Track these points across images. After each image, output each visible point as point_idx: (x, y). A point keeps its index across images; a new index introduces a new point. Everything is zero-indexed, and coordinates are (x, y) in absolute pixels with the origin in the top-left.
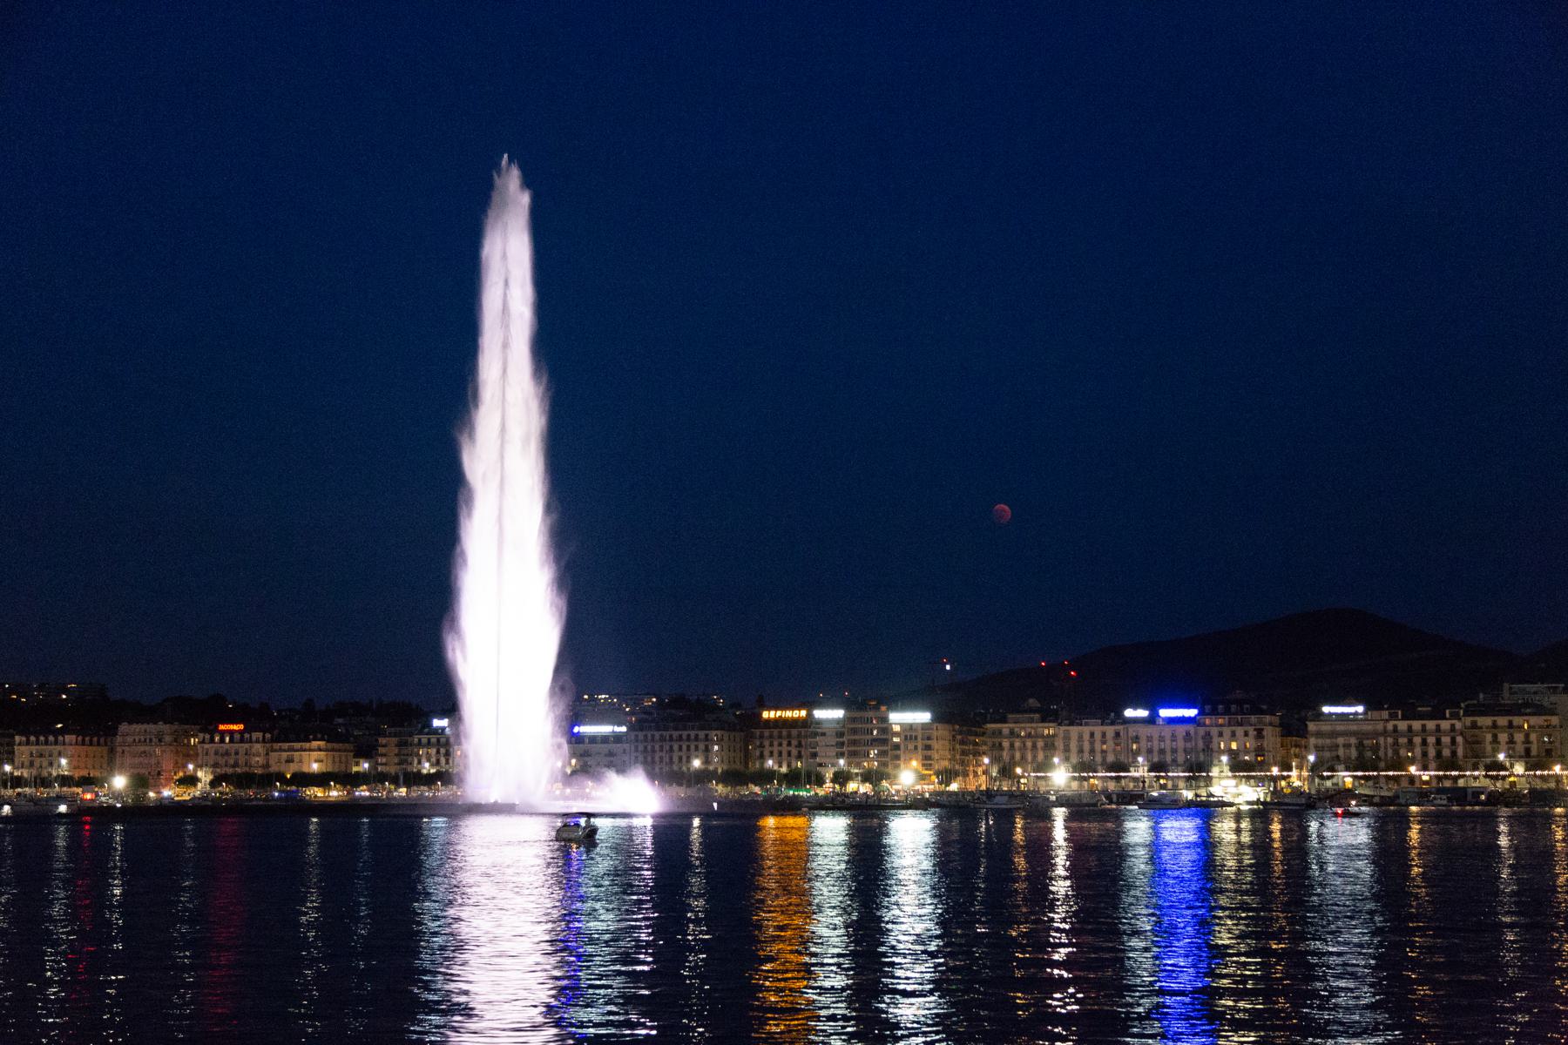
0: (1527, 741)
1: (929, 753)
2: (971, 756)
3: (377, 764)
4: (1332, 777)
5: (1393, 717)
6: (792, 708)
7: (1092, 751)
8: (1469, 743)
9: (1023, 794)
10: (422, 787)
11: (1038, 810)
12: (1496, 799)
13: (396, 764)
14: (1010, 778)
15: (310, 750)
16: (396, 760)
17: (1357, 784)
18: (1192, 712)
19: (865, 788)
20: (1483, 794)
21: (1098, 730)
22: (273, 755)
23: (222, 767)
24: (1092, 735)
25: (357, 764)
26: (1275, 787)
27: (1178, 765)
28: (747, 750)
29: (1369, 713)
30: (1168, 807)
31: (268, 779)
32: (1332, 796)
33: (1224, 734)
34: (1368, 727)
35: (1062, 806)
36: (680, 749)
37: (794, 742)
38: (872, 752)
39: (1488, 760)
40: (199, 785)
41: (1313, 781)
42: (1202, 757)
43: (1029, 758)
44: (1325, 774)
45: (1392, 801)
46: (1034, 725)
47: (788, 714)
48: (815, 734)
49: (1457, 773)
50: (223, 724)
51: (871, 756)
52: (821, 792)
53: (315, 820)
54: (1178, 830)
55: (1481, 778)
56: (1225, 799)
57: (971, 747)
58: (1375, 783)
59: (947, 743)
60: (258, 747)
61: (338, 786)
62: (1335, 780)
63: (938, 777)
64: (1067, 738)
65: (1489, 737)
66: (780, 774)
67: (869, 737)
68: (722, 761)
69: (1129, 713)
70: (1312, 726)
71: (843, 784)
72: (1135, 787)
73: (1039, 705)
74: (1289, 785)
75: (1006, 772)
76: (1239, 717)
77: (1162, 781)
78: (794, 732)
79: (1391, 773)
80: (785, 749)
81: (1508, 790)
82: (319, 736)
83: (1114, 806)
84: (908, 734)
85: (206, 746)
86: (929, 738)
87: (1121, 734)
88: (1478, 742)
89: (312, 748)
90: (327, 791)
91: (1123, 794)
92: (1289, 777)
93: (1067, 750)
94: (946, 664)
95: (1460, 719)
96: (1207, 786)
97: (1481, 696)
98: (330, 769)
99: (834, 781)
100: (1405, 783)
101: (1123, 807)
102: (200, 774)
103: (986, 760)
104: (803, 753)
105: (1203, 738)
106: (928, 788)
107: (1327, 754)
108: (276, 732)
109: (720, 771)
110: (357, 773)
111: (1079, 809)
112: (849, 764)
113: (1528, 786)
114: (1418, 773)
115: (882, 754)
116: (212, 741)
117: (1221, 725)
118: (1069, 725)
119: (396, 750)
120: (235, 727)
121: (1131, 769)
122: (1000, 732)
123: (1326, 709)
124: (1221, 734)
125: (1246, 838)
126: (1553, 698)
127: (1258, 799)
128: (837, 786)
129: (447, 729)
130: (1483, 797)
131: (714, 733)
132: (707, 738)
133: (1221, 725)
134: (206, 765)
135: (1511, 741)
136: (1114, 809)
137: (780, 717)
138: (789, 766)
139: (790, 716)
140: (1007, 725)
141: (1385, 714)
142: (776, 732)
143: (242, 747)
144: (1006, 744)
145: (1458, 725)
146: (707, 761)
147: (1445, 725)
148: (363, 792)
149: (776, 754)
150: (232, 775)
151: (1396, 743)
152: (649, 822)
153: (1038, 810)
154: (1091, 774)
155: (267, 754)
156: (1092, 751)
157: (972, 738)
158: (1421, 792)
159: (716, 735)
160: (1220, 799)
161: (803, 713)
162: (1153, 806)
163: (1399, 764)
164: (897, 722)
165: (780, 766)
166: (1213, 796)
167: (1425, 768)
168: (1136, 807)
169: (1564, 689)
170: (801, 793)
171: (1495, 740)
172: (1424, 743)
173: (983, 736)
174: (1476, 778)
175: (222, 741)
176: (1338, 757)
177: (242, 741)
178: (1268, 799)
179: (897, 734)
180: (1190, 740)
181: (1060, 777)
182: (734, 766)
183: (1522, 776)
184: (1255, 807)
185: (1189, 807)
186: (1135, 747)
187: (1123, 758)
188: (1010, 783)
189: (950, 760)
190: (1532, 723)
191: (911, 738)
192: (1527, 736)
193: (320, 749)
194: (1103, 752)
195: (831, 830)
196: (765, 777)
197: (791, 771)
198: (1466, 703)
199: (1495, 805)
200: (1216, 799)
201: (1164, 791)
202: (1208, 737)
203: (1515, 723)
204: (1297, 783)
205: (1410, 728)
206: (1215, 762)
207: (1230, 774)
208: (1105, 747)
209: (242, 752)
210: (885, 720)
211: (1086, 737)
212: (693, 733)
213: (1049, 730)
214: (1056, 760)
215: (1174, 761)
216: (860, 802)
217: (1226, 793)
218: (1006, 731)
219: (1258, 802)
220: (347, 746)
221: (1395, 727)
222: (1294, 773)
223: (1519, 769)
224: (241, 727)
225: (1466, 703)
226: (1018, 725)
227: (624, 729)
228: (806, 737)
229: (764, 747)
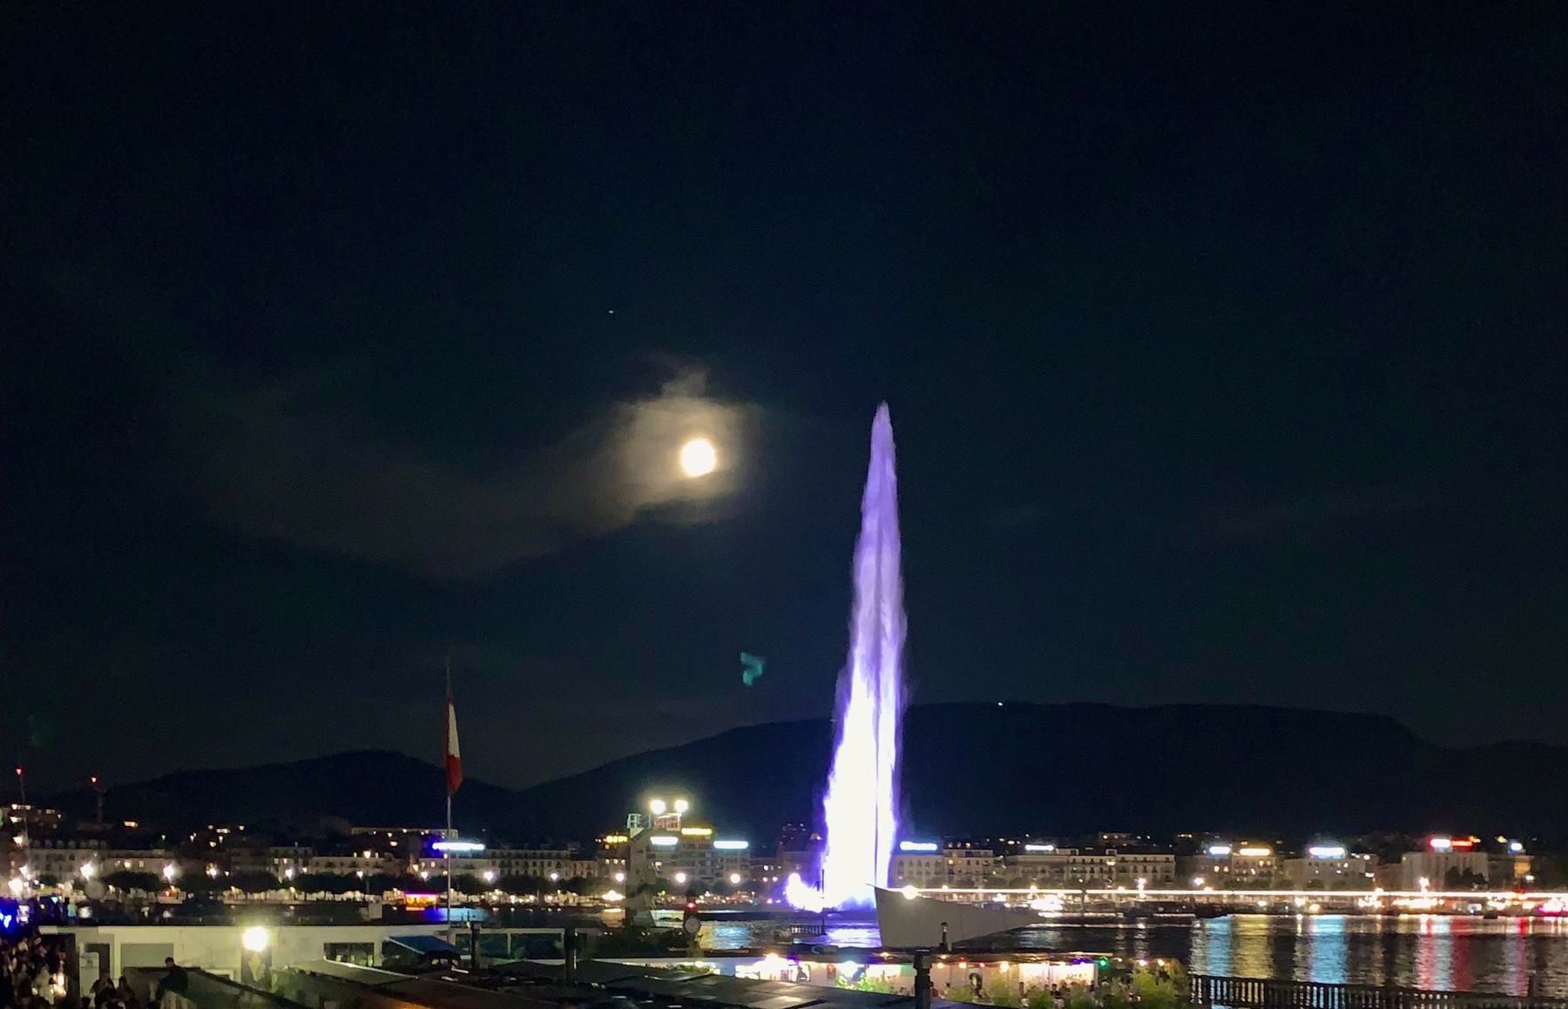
5: (1073, 854)
33: (971, 863)
34: (1057, 859)
36: (535, 864)
65: (1132, 868)
141: (1068, 851)
229: (528, 866)
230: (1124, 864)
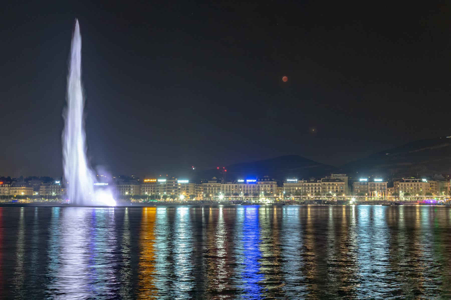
0: (337, 188)
1: (188, 191)
2: (199, 192)
3: (40, 193)
4: (289, 197)
5: (305, 182)
6: (152, 179)
7: (230, 190)
8: (323, 189)
9: (212, 201)
10: (52, 199)
11: (216, 206)
12: (329, 203)
13: (45, 193)
14: (208, 197)
16: (45, 192)
17: (295, 199)
18: (255, 181)
19: (171, 200)
20: (326, 201)
21: (231, 185)
24: (230, 186)
25: (34, 193)
26: (275, 200)
29: (299, 181)
32: (289, 202)
37: (153, 188)
38: (173, 190)
39: (327, 193)
41: (284, 198)
42: (257, 192)
43: (214, 192)
44: (287, 196)
45: (304, 203)
46: (215, 184)
47: (151, 180)
48: (158, 186)
49: (320, 196)
52: (159, 200)
54: (251, 210)
55: (326, 197)
57: (199, 189)
58: (300, 199)
59: (192, 188)
60: (7, 188)
61: (29, 199)
62: (290, 198)
64: (223, 187)
65: (328, 187)
66: (149, 196)
68: (134, 193)
69: (239, 181)
70: (284, 184)
71: (165, 199)
73: (217, 179)
74: (279, 199)
75: (208, 196)
76: (267, 182)
77: (247, 198)
78: (153, 185)
79: (303, 196)
80: (150, 190)
81: (332, 200)
82: (24, 185)
86: (188, 187)
87: (237, 186)
88: (325, 189)
89: (22, 189)
92: (279, 197)
93: (223, 190)
94: (193, 168)
95: (321, 183)
96: (258, 199)
97: (326, 177)
98: (27, 194)
99: (163, 198)
100: (307, 198)
104: (155, 190)
105: (258, 187)
107: (288, 191)
109: (133, 195)
110: (34, 195)
111: (227, 205)
112: (167, 194)
113: (337, 199)
114: (310, 196)
115: (176, 191)
117: (262, 184)
119: (45, 189)
121: (239, 195)
123: (288, 180)
124: (262, 186)
125: (268, 213)
126: (343, 178)
127: (271, 203)
129: (59, 184)
130: (326, 202)
132: (130, 187)
133: (262, 184)
135: (333, 188)
136: (235, 205)
137: (149, 181)
138: (151, 194)
140: (207, 184)
141: (303, 181)
144: (208, 188)
145: (320, 184)
146: (130, 193)
147: (317, 184)
148: (36, 200)
151: (305, 189)
153: (216, 206)
154: (229, 196)
155: (9, 190)
156: (230, 190)
158: (311, 201)
159: (132, 186)
161: (155, 180)
163: (305, 194)
165: (149, 194)
166: (260, 202)
167: (312, 195)
168: (240, 205)
169: (346, 175)
170: (154, 201)
171: (329, 188)
172: (312, 189)
174: (324, 198)
176: (291, 192)
178: (273, 203)
179: (180, 186)
181: (221, 197)
183: (335, 197)
184: (270, 205)
186: (240, 189)
187: (237, 192)
189: (193, 192)
190: (338, 184)
191: (183, 187)
192: (337, 187)
193: (24, 189)
195: (162, 212)
196: (144, 197)
197: (152, 195)
198: (322, 179)
199: (328, 204)
200: (260, 203)
202: (259, 187)
203: (334, 184)
204: (281, 199)
205: (309, 185)
206: (261, 193)
207: (264, 196)
208: (233, 189)
210: (176, 182)
211: (228, 187)
213: (218, 184)
214: (220, 193)
215: (250, 193)
218: (208, 185)
219: (271, 203)
220: (31, 188)
221: (305, 185)
222: (280, 196)
223: (335, 195)
225: (322, 179)
226: (210, 184)
230: (324, 186)
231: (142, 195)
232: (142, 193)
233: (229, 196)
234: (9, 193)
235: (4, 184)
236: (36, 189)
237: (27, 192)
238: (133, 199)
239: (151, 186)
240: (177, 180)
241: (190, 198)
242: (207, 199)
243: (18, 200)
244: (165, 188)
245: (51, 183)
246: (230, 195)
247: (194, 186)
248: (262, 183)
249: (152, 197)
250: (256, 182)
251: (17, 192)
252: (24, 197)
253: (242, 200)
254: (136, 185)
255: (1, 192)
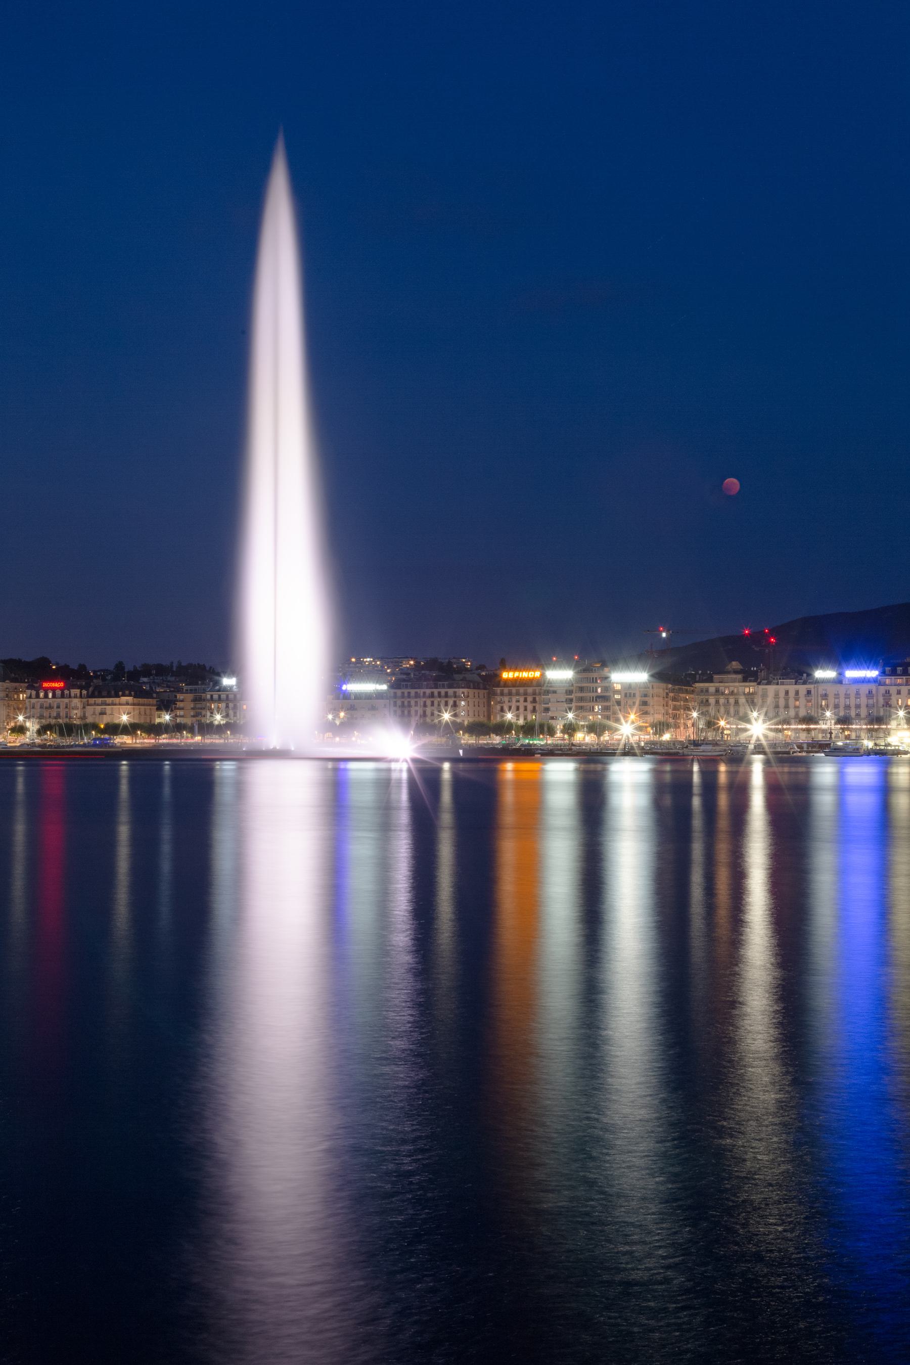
1: (645, 708)
6: (528, 670)
7: (787, 707)
15: (120, 704)
16: (192, 714)
21: (792, 688)
22: (90, 710)
23: (63, 718)
24: (787, 693)
25: (159, 717)
27: (861, 719)
28: (489, 705)
30: (849, 754)
31: (88, 727)
35: (759, 753)
36: (432, 704)
37: (530, 699)
38: (596, 707)
40: (28, 733)
42: (882, 714)
46: (737, 684)
47: (525, 675)
48: (547, 692)
50: (46, 682)
51: (596, 710)
53: (124, 762)
56: (901, 748)
57: (682, 703)
60: (76, 702)
61: (143, 735)
63: (652, 729)
66: (517, 726)
67: (594, 695)
69: (820, 674)
72: (823, 737)
73: (742, 668)
75: (710, 724)
78: (530, 690)
80: (522, 704)
82: (127, 692)
83: (804, 754)
84: (628, 692)
85: (33, 701)
86: (646, 696)
87: (812, 692)
90: (134, 738)
91: (813, 744)
94: (662, 632)
98: (135, 721)
99: (564, 731)
101: (812, 754)
102: (28, 724)
103: (695, 714)
104: (537, 708)
105: (883, 696)
106: (647, 737)
108: (91, 689)
109: (466, 723)
110: (160, 724)
115: (606, 708)
116: (38, 696)
117: (899, 685)
118: (767, 684)
120: (56, 685)
122: (707, 691)
124: (899, 693)
128: (566, 736)
131: (462, 690)
133: (899, 685)
134: (33, 717)
137: (518, 677)
138: (525, 719)
139: (526, 676)
142: (514, 690)
143: (47, 702)
144: (712, 700)
146: (455, 715)
149: (514, 708)
150: (55, 725)
152: (405, 766)
154: (785, 727)
155: (84, 707)
156: (787, 707)
157: (682, 695)
159: (463, 693)
160: (897, 748)
161: (537, 674)
162: (839, 754)
164: (619, 681)
168: (823, 755)
170: (535, 742)
173: (692, 694)
175: (46, 696)
177: (63, 696)
179: (618, 692)
180: (872, 697)
182: (477, 719)
185: (869, 754)
187: (813, 713)
188: (714, 733)
191: (630, 696)
193: (127, 704)
194: (796, 707)
196: (503, 729)
197: (526, 723)
200: (893, 748)
201: (848, 741)
207: (906, 726)
208: (797, 703)
209: (62, 706)
211: (782, 694)
212: (443, 691)
213: (750, 688)
215: (858, 715)
216: (585, 749)
217: (902, 743)
218: (712, 689)
220: (151, 701)
224: (62, 684)
227: (384, 687)
228: (540, 694)
231: (495, 722)
232: (495, 717)
233: (785, 727)
234: (84, 717)
235: (68, 690)
236: (166, 705)
237: (137, 712)
238: (467, 736)
239: (526, 694)
240: (610, 672)
241: (651, 731)
242: (710, 736)
243: (110, 739)
244: (571, 700)
245: (209, 684)
246: (789, 723)
247: (667, 691)
248: (899, 681)
249: (529, 730)
250: (876, 678)
251: (108, 712)
252: (129, 729)
253: (831, 737)
254: (476, 691)
255: (61, 714)
